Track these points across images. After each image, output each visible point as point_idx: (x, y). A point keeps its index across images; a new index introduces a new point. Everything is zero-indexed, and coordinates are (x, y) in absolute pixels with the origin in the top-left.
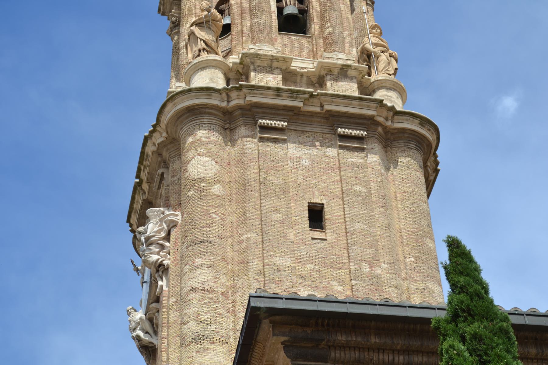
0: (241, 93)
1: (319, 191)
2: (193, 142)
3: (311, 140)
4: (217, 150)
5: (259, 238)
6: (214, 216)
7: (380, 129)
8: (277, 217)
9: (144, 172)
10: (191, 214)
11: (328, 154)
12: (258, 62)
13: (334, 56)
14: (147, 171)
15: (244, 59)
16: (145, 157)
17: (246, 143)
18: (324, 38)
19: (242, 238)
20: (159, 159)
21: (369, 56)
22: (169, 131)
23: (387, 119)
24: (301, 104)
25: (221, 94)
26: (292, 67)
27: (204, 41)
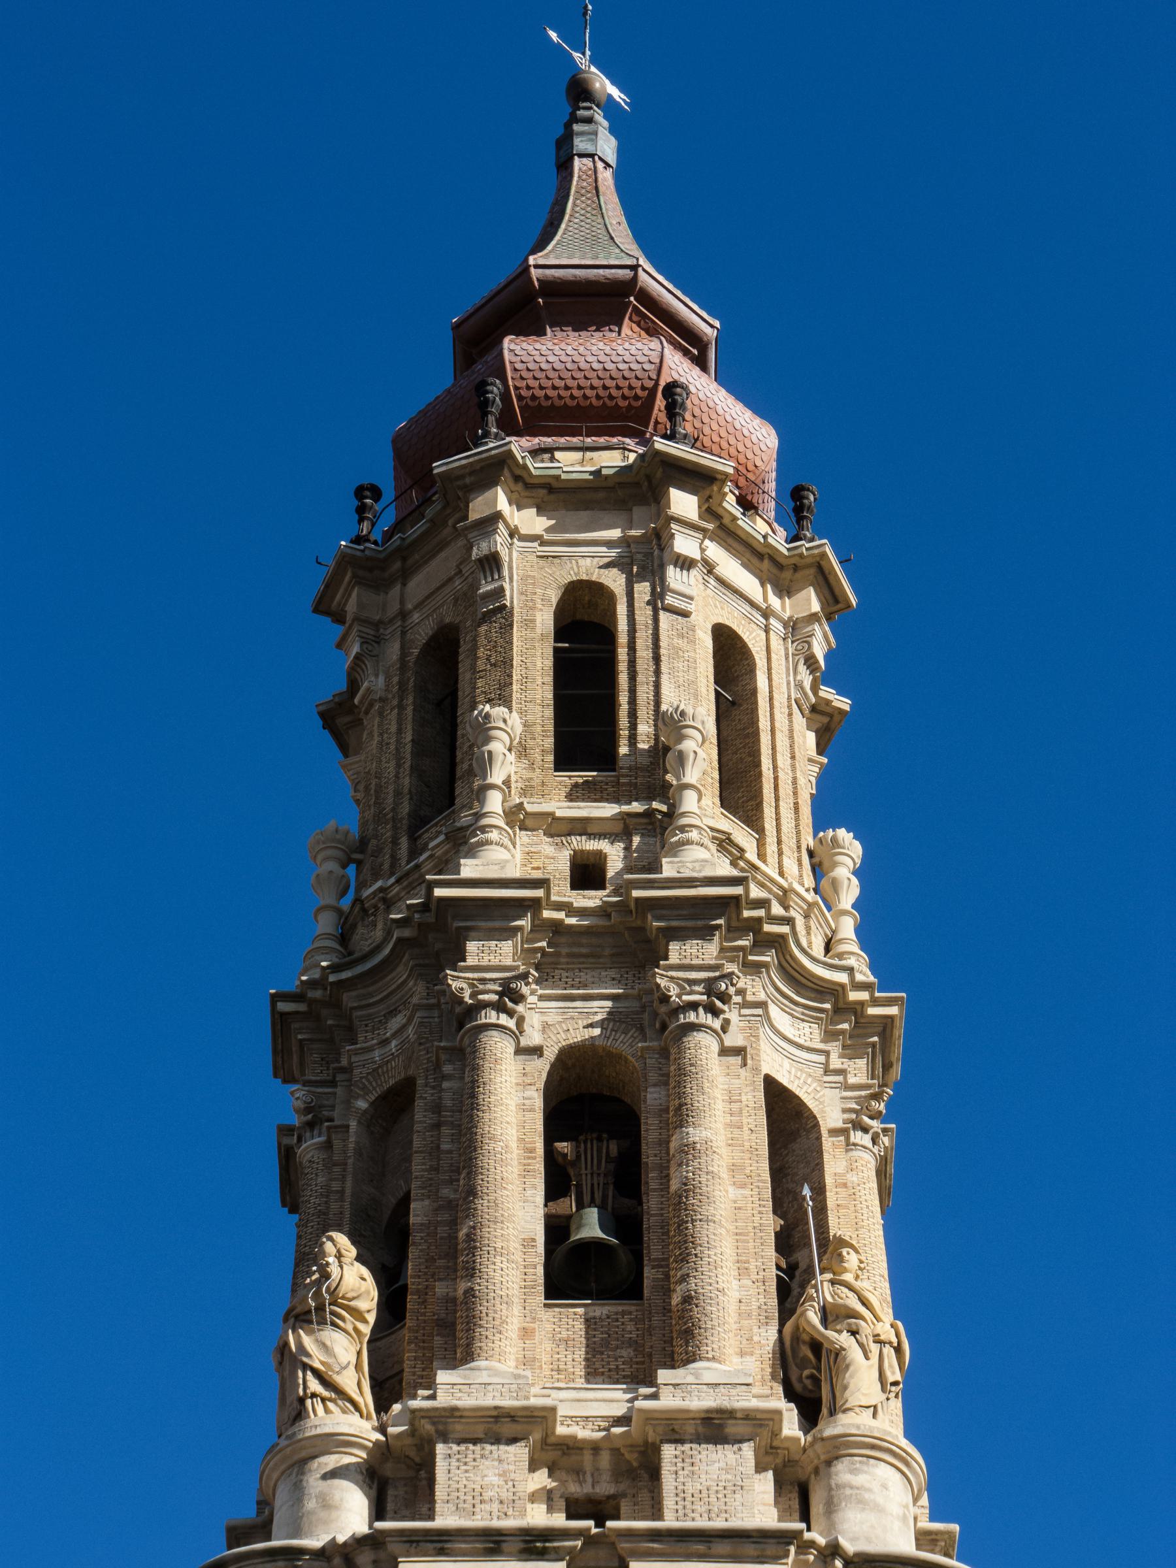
0: (382, 1555)
12: (458, 1428)
13: (690, 1379)
15: (417, 1423)
21: (816, 1346)
25: (329, 1559)
26: (561, 1430)
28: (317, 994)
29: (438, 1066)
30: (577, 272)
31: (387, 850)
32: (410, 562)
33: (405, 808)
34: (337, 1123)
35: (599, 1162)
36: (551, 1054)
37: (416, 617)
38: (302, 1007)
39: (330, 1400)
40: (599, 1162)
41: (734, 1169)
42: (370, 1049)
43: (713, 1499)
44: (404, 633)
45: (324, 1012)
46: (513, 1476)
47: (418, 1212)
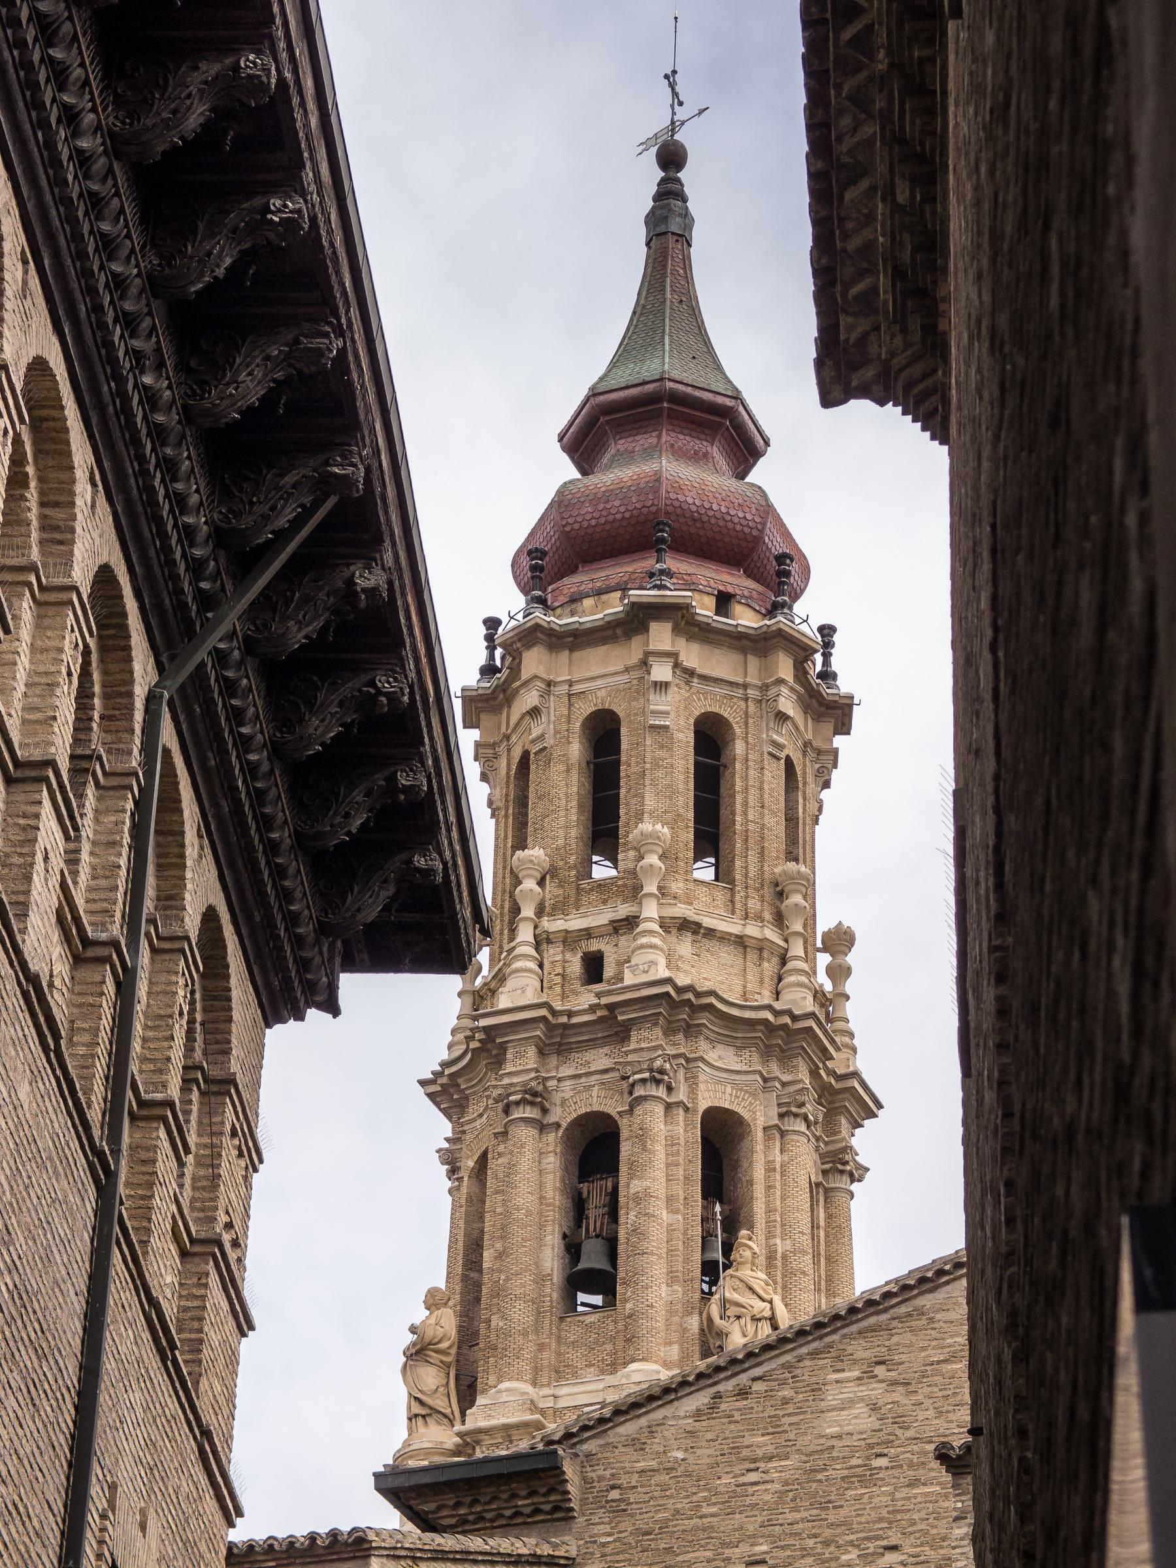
32: (509, 692)
36: (564, 1124)
37: (514, 738)
39: (429, 1415)
41: (670, 1200)
42: (474, 1120)
44: (509, 750)
45: (451, 1090)
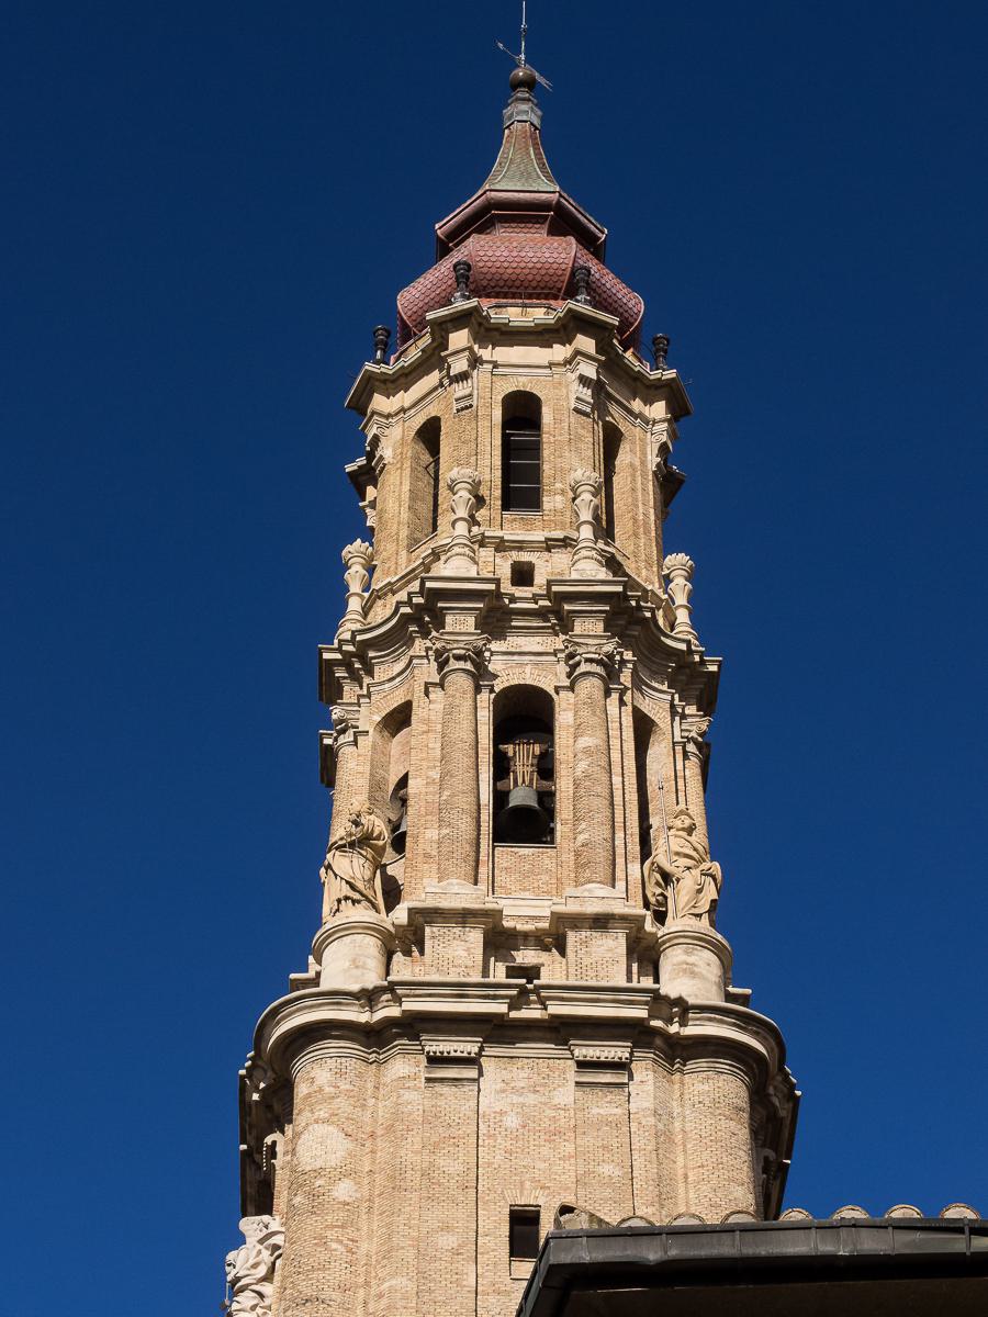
1: (533, 1180)
2: (309, 1095)
3: (526, 1075)
4: (349, 1109)
5: (412, 1287)
6: (334, 1246)
7: (658, 1041)
8: (448, 1241)
9: (250, 1134)
10: (295, 1242)
11: (556, 1101)
13: (586, 894)
14: (254, 1132)
16: (247, 1109)
17: (402, 1092)
18: (577, 854)
19: (382, 1288)
20: (269, 1116)
22: (276, 1067)
23: (670, 1021)
24: (500, 1008)
27: (347, 882)
28: (351, 648)
29: (427, 694)
30: (516, 194)
31: (393, 559)
33: (404, 533)
34: (360, 729)
35: (528, 757)
38: (339, 656)
40: (528, 757)
43: (599, 968)
46: (472, 950)
47: (414, 786)
